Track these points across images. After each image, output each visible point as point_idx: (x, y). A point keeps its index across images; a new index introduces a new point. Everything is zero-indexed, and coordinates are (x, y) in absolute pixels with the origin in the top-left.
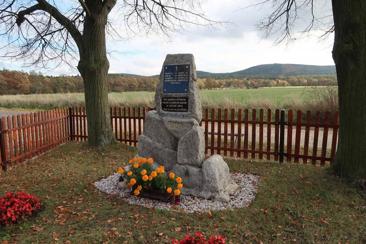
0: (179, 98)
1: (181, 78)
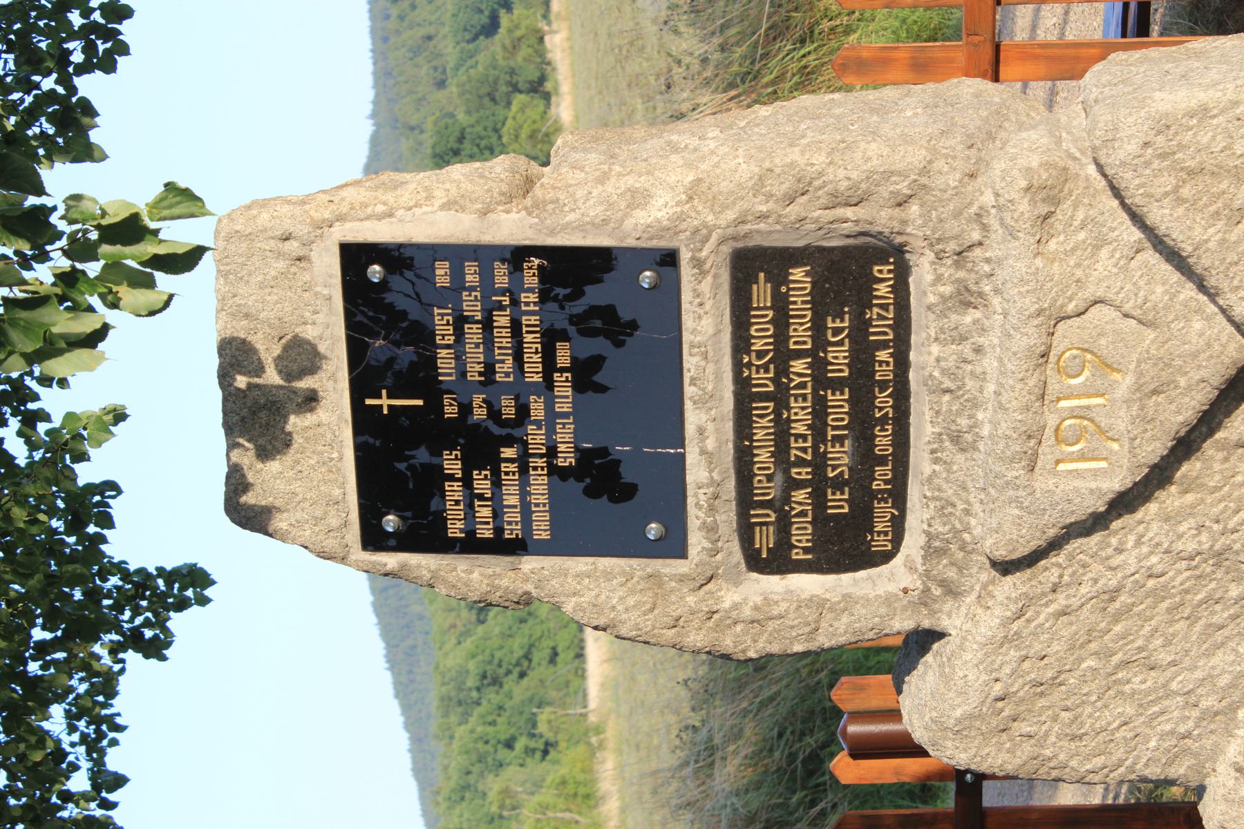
0: (738, 366)
1: (503, 338)
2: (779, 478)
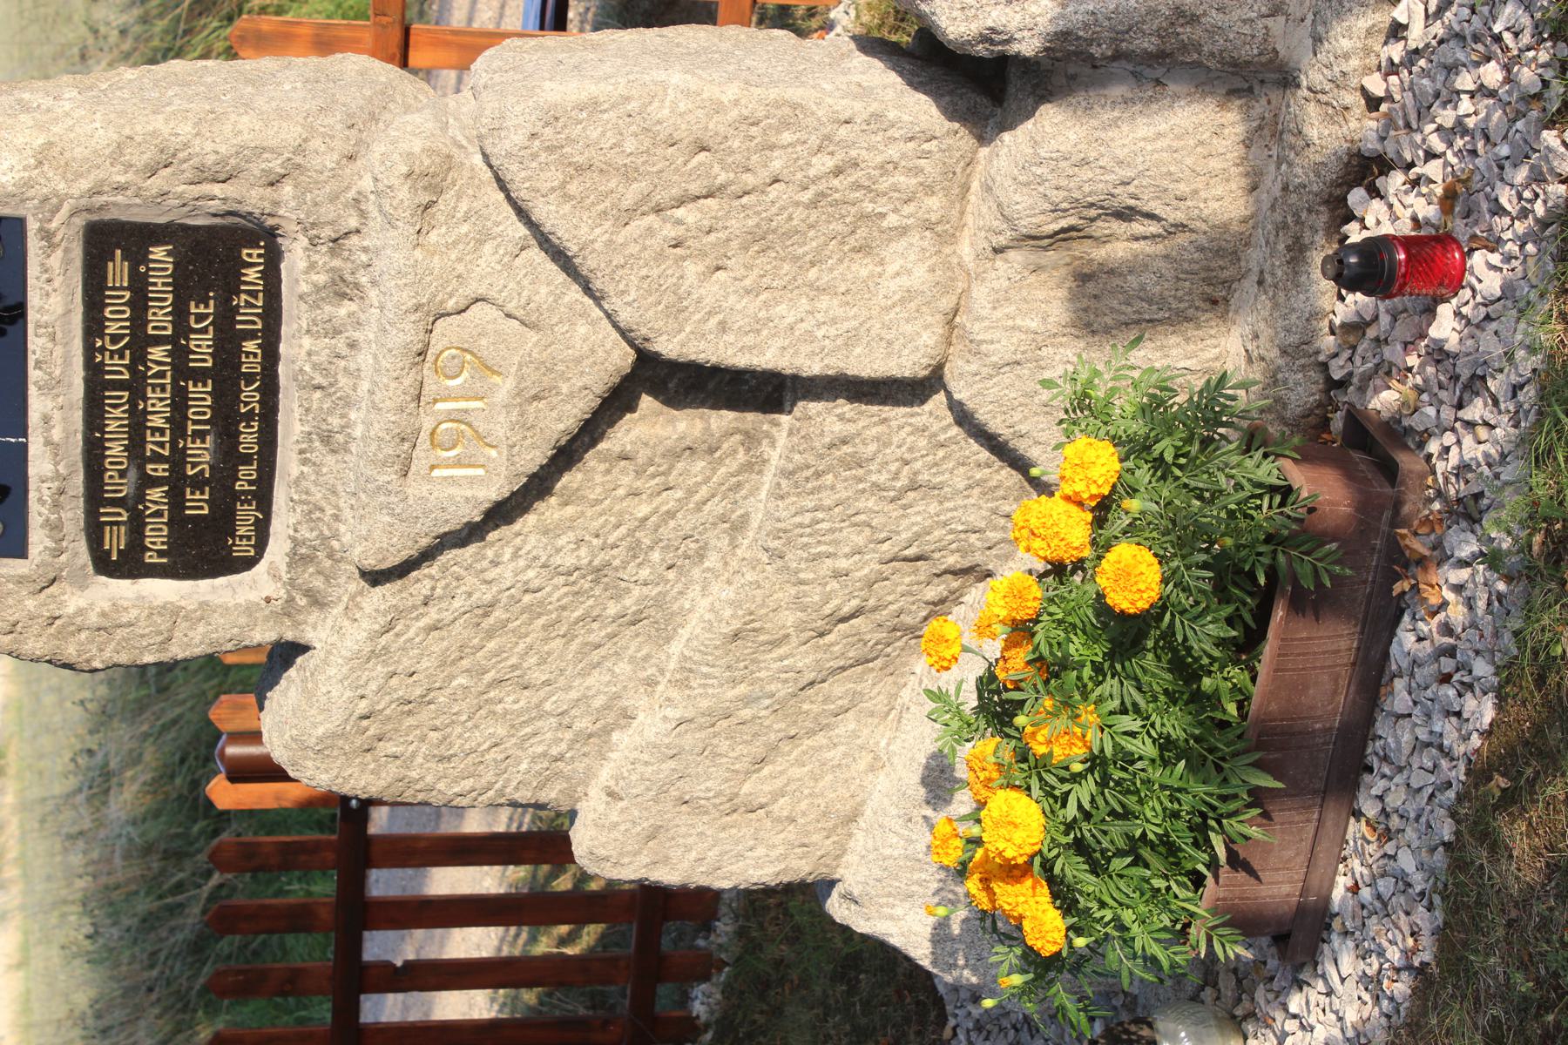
0: (90, 350)
2: (133, 475)
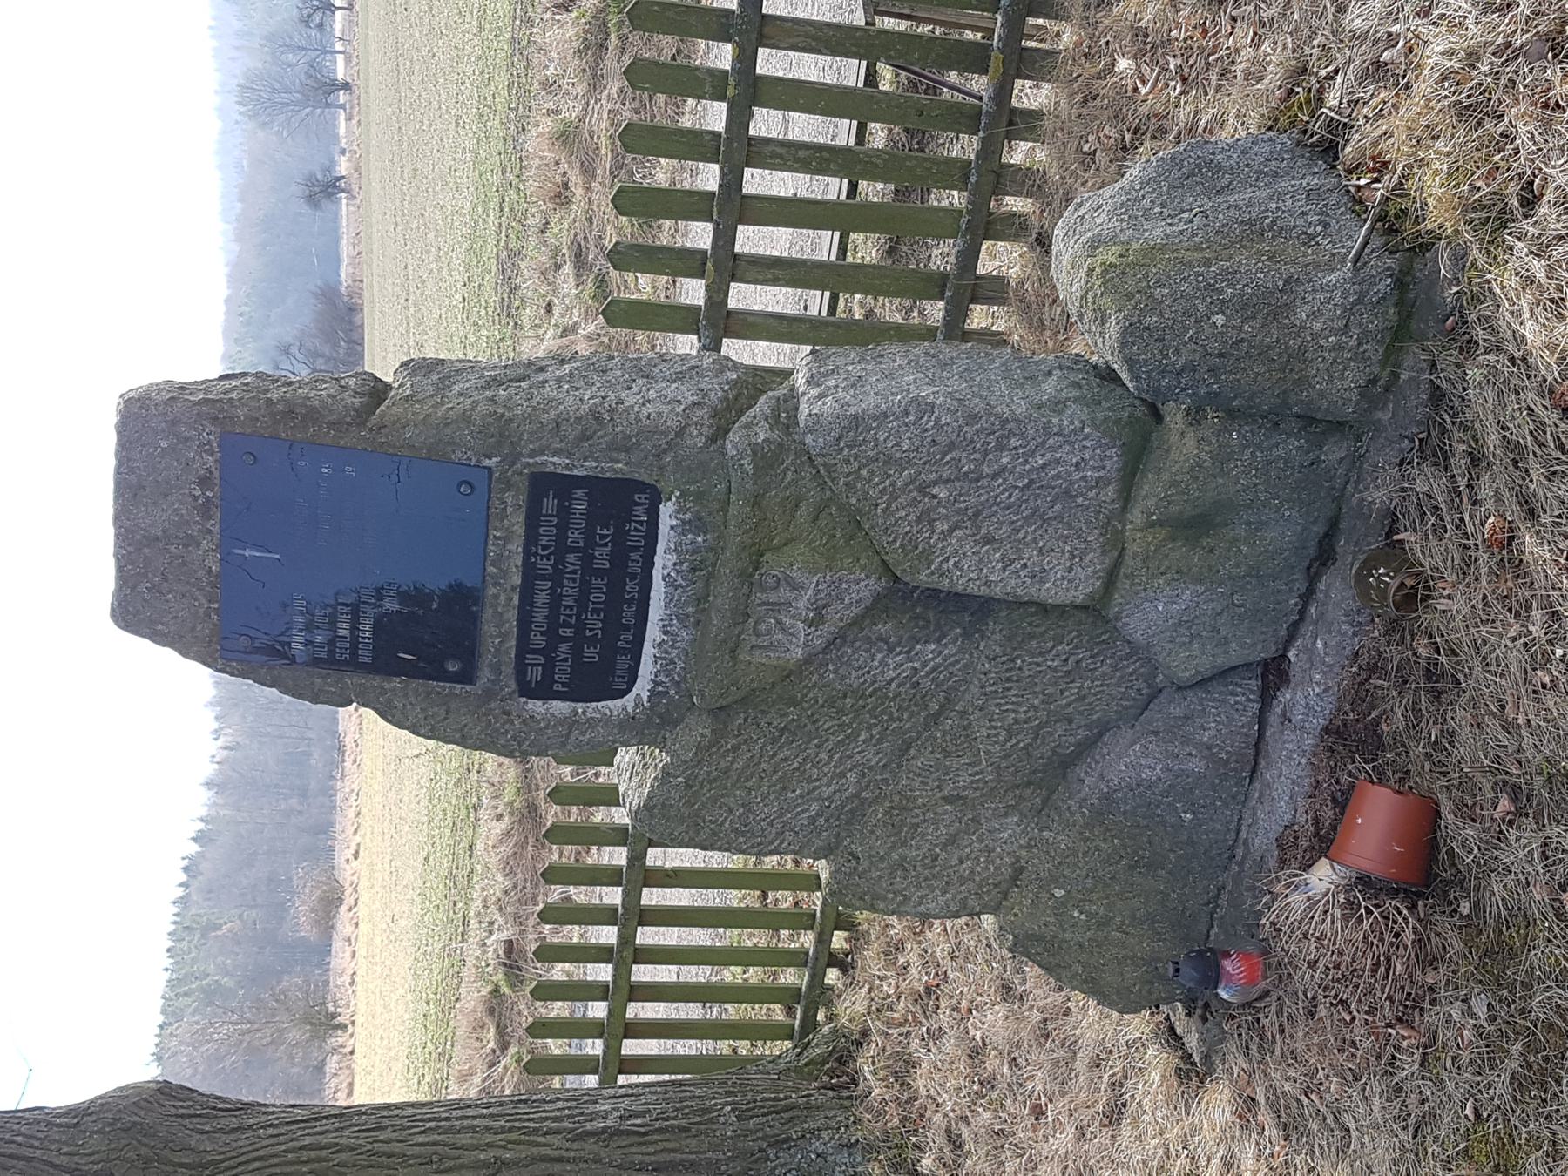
0: (527, 553)
